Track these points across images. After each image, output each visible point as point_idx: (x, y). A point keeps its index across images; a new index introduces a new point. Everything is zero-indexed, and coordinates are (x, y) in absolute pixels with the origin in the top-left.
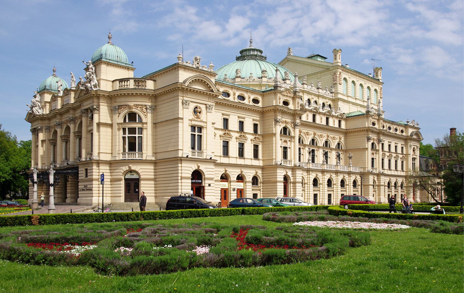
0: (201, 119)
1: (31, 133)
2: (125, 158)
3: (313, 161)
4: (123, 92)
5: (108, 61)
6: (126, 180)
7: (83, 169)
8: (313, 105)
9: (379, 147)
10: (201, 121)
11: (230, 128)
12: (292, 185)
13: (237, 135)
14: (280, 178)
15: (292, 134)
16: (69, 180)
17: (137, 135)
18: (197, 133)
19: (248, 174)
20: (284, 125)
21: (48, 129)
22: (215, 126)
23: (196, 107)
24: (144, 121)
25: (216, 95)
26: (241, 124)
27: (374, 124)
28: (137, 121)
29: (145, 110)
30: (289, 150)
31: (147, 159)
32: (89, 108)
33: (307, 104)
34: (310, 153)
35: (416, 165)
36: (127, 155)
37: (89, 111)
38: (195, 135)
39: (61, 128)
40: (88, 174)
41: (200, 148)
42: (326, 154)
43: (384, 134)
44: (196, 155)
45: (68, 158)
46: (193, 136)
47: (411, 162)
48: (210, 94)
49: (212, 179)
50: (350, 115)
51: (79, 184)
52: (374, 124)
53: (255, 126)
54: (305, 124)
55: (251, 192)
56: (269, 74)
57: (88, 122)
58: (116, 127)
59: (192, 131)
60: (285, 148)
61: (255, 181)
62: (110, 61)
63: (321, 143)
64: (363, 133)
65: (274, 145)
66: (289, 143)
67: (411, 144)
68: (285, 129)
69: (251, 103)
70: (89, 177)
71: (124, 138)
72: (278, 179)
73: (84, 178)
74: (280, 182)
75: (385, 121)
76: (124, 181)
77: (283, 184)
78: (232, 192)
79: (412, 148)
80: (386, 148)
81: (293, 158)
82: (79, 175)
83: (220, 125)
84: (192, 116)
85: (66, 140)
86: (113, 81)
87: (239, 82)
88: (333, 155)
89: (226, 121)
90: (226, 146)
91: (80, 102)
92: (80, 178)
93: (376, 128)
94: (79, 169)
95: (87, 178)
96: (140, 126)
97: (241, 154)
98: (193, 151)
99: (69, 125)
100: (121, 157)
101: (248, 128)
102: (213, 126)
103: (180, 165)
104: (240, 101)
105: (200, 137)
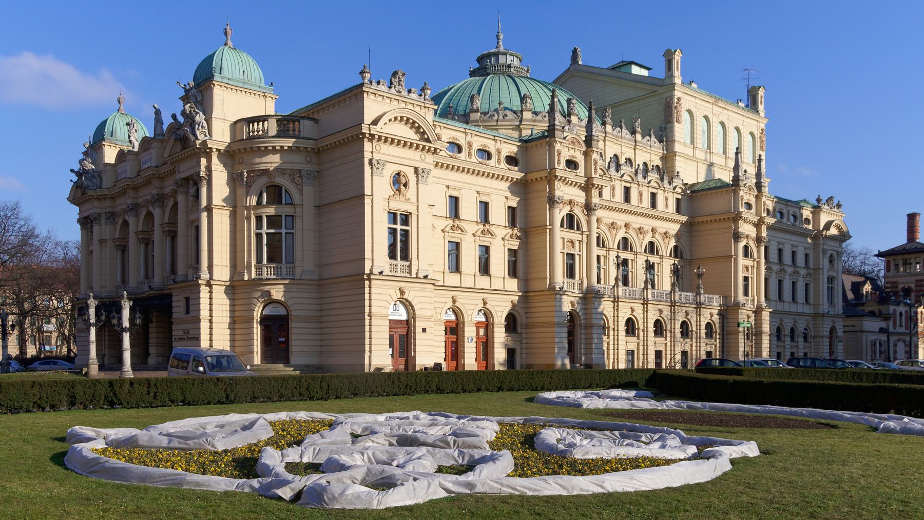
1: (79, 226)
3: (626, 283)
8: (626, 169)
11: (462, 215)
12: (583, 331)
17: (283, 231)
18: (399, 227)
19: (497, 309)
20: (566, 210)
21: (112, 216)
22: (434, 211)
24: (297, 199)
26: (485, 206)
29: (297, 179)
33: (613, 165)
35: (835, 291)
37: (191, 182)
41: (405, 256)
44: (399, 270)
46: (393, 232)
47: (826, 285)
49: (428, 318)
56: (536, 104)
57: (190, 205)
59: (389, 223)
63: (640, 244)
64: (725, 225)
66: (577, 244)
67: (826, 247)
69: (504, 165)
71: (259, 236)
79: (828, 256)
89: (455, 202)
96: (288, 210)
97: (485, 268)
98: (393, 262)
102: (430, 210)
105: (406, 234)
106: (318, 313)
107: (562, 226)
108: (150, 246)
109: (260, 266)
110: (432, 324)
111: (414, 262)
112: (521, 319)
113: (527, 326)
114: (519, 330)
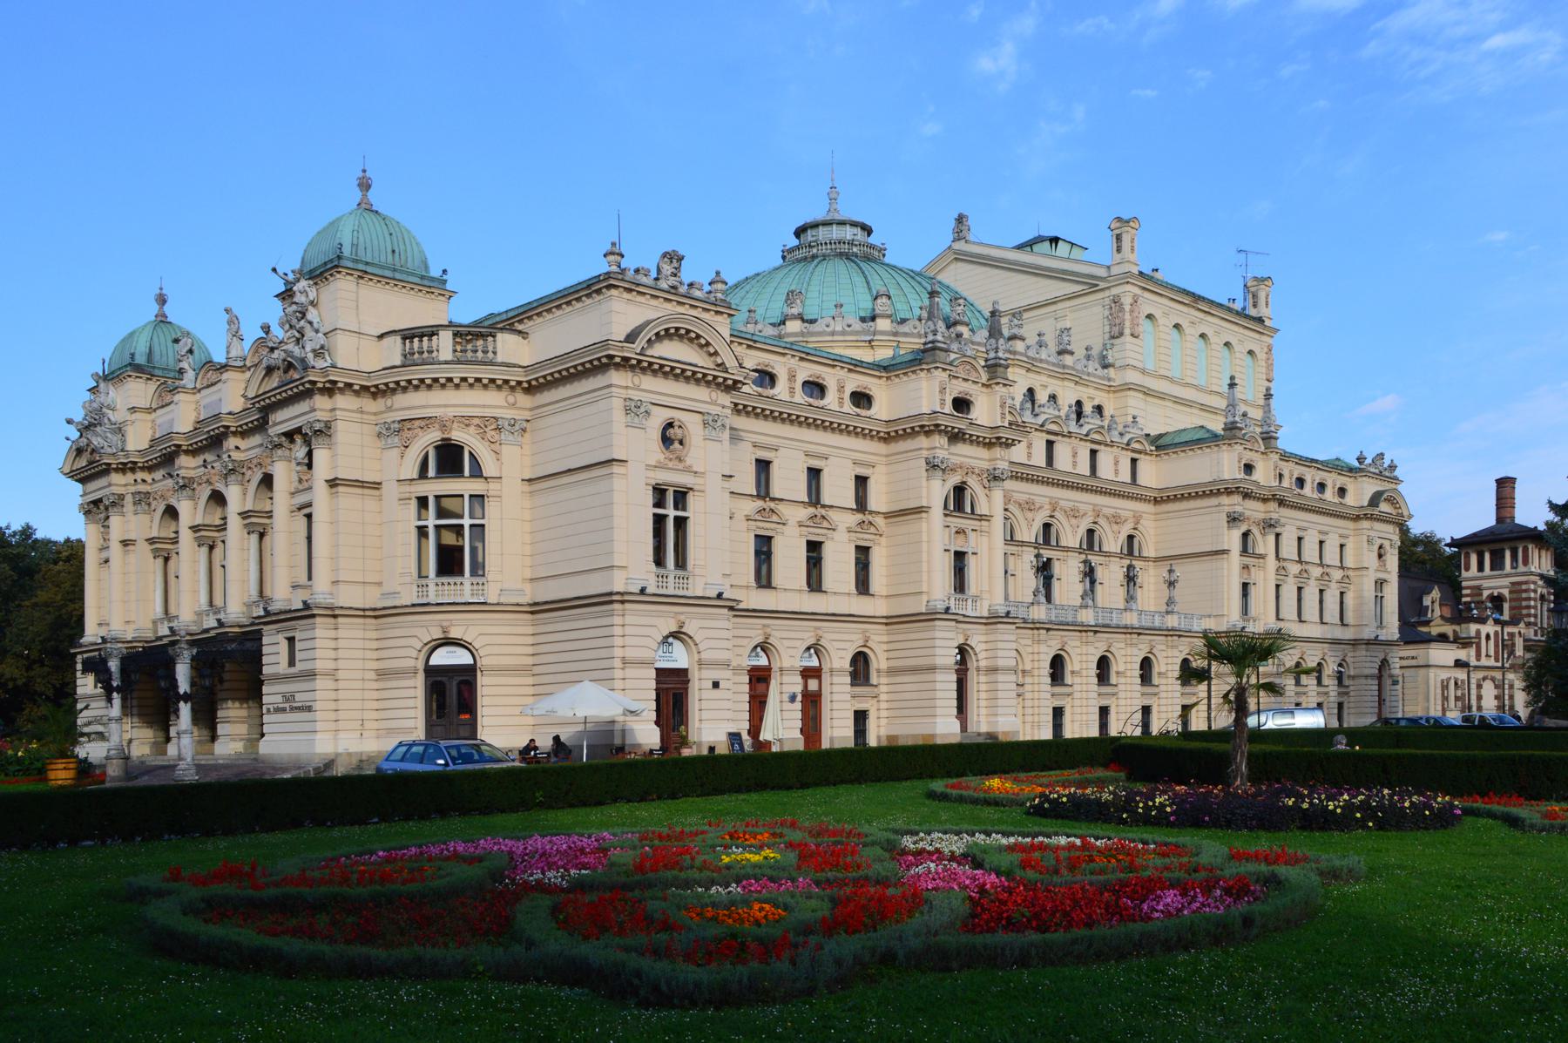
0: (689, 461)
1: (82, 517)
2: (424, 601)
4: (415, 374)
5: (361, 267)
6: (431, 671)
7: (281, 639)
9: (1265, 544)
10: (687, 470)
12: (983, 679)
13: (805, 513)
14: (949, 657)
15: (982, 509)
16: (226, 676)
17: (466, 522)
18: (671, 512)
22: (733, 485)
23: (670, 425)
24: (489, 468)
25: (736, 382)
26: (814, 474)
27: (1249, 468)
28: (467, 473)
29: (490, 434)
30: (971, 562)
31: (502, 600)
32: (298, 430)
34: (1038, 570)
36: (432, 587)
38: (666, 516)
39: (192, 498)
40: (299, 656)
41: (681, 563)
42: (1089, 573)
43: (1282, 503)
45: (218, 602)
46: (659, 521)
48: (715, 377)
50: (1161, 442)
51: (265, 689)
52: (1249, 468)
53: (861, 481)
54: (1022, 475)
55: (848, 706)
58: (391, 491)
60: (960, 556)
61: (860, 667)
62: (369, 269)
63: (1071, 536)
64: (1214, 501)
65: (925, 546)
66: (972, 535)
67: (1372, 533)
68: (959, 490)
70: (299, 667)
71: (422, 532)
72: (939, 661)
73: (283, 667)
74: (945, 668)
75: (1285, 456)
76: (421, 676)
77: (954, 677)
78: (787, 706)
79: (1376, 547)
80: (1288, 550)
81: (986, 587)
82: (265, 660)
83: (747, 481)
84: (656, 452)
85: (210, 539)
86: (381, 337)
87: (795, 335)
88: (1111, 574)
89: (763, 466)
90: (764, 549)
91: (261, 410)
92: (266, 670)
93: (1256, 483)
94: (265, 640)
95: (293, 670)
96: (476, 486)
98: (662, 571)
99: (220, 486)
100: (409, 596)
101: (838, 490)
102: (726, 485)
103: (617, 620)
104: (811, 400)
105: (681, 523)
106: (530, 661)
107: (946, 507)
108: (218, 552)
109: (424, 582)
110: (728, 674)
111: (697, 571)
112: (879, 662)
113: (892, 672)
114: (874, 680)
